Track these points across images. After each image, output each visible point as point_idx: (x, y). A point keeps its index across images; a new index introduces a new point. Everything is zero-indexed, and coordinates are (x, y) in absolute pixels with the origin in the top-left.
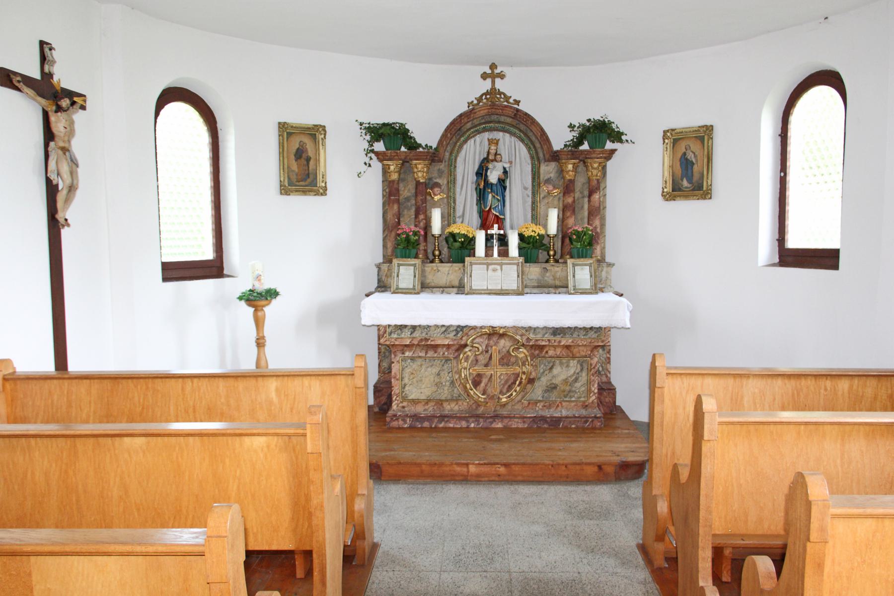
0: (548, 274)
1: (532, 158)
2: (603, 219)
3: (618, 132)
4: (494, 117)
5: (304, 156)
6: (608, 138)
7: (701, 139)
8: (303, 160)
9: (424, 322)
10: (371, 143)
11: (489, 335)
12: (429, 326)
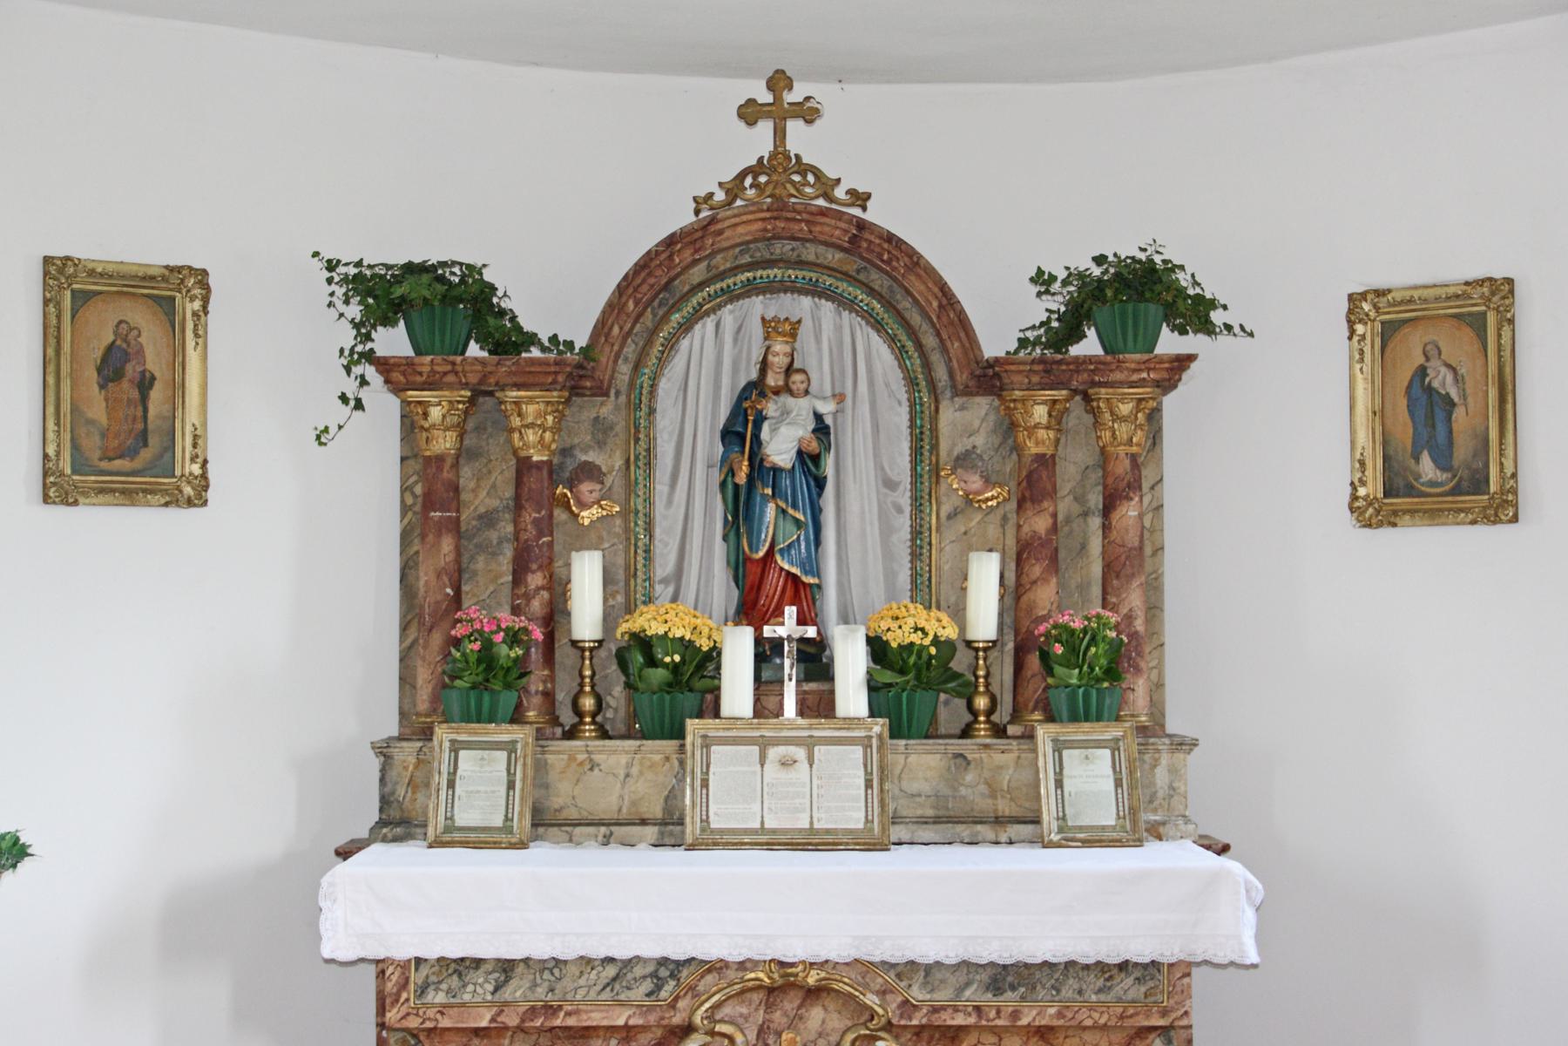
0: (969, 778)
1: (911, 382)
2: (1154, 588)
3: (1199, 299)
4: (782, 248)
5: (131, 370)
6: (1166, 318)
7: (1477, 324)
8: (125, 384)
9: (541, 949)
10: (363, 329)
11: (771, 990)
12: (558, 962)
